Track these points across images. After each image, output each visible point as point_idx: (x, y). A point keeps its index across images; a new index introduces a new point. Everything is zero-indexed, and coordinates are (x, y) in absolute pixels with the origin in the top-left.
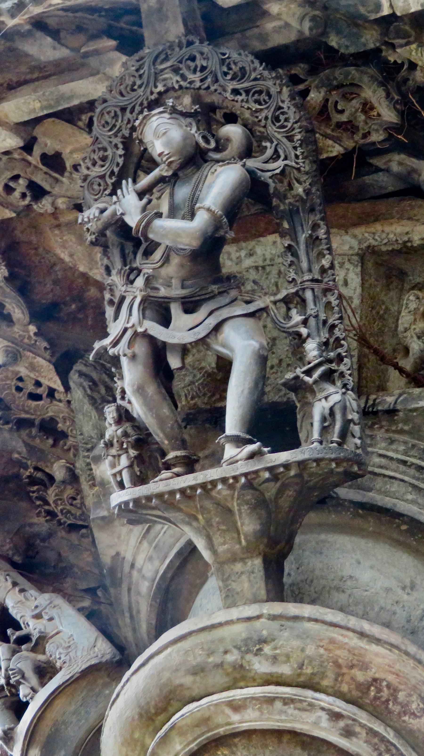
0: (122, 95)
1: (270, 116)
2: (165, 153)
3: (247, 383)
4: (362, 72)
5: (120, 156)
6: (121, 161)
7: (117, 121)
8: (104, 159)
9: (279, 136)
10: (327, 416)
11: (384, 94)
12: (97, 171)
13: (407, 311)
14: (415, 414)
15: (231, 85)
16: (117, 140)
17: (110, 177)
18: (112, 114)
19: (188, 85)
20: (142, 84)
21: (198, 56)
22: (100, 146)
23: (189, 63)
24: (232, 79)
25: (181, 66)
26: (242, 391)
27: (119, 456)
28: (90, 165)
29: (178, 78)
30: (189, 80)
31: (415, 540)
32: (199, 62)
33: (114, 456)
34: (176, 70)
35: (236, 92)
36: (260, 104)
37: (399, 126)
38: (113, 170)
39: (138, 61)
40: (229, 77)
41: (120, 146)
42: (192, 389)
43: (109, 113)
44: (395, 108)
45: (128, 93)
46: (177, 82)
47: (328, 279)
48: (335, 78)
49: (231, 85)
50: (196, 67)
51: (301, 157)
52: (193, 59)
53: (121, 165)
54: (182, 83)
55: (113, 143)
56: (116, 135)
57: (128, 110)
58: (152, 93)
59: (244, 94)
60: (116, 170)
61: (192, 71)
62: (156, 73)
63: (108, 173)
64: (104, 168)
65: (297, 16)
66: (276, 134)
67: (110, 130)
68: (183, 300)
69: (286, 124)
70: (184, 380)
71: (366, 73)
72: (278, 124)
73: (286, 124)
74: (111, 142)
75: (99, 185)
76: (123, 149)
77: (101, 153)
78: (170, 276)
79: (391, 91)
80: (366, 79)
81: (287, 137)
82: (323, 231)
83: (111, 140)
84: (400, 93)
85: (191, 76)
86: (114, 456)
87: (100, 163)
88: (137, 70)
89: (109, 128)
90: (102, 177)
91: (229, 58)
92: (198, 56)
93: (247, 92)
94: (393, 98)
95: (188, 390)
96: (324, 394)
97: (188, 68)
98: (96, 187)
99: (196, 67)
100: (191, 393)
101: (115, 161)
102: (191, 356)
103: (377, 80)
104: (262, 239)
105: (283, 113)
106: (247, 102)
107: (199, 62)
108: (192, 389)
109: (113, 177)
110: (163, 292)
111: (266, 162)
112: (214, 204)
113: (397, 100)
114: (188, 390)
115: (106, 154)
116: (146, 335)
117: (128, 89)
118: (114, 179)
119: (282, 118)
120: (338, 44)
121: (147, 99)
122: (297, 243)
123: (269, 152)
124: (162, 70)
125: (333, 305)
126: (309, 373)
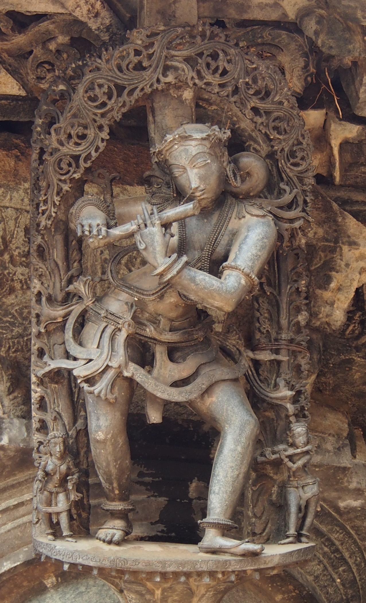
0: (120, 69)
1: (286, 149)
2: (200, 189)
3: (244, 467)
4: (292, 38)
5: (103, 140)
6: (102, 146)
7: (110, 98)
8: (83, 137)
9: (291, 175)
10: (303, 507)
11: (303, 64)
12: (69, 149)
13: (119, 192)
14: (317, 469)
15: (254, 102)
16: (104, 122)
17: (85, 161)
18: (105, 89)
19: (203, 86)
20: (150, 66)
21: (221, 55)
22: (81, 121)
23: (209, 59)
24: (255, 94)
25: (200, 61)
26: (238, 475)
27: (57, 493)
28: (63, 137)
29: (195, 75)
30: (205, 81)
31: (272, 587)
32: (222, 63)
33: (51, 493)
34: (187, 60)
35: (255, 110)
36: (279, 133)
37: (300, 97)
38: (90, 153)
39: (148, 36)
40: (251, 92)
41: (107, 130)
42: (19, 342)
43: (100, 86)
44: (306, 79)
45: (128, 69)
46: (192, 78)
47: (301, 339)
48: (262, 37)
49: (254, 102)
50: (217, 68)
51: (310, 205)
52: (215, 56)
53: (100, 151)
54: (197, 81)
55: (98, 124)
56: (103, 115)
57: (126, 91)
58: (158, 81)
59: (264, 117)
60: (94, 154)
61: (211, 71)
62: (166, 57)
63: (83, 156)
64: (80, 148)
65: (297, 7)
66: (288, 170)
67: (97, 107)
68: (170, 345)
69: (301, 162)
70: (12, 331)
71: (296, 41)
72: (292, 160)
73: (301, 162)
74: (95, 121)
75: (70, 165)
76: (109, 134)
77: (80, 130)
78: (159, 312)
79: (311, 63)
80: (293, 46)
81: (297, 177)
82: (303, 282)
83: (97, 119)
84: (318, 66)
85: (209, 78)
86: (51, 493)
87: (75, 139)
88: (146, 47)
89: (95, 104)
90: (76, 158)
91: (255, 69)
92: (221, 55)
93: (268, 113)
94: (309, 71)
95: (14, 342)
96: (301, 483)
97: (208, 65)
98: (64, 166)
99: (217, 68)
100: (16, 346)
101: (96, 144)
102: (14, 297)
103: (303, 49)
104: (128, 187)
105: (303, 150)
106: (267, 126)
107: (222, 63)
108: (19, 342)
109: (89, 162)
110: (150, 331)
111: (281, 208)
112: (252, 268)
113: (312, 74)
114: (14, 342)
115: (86, 132)
116: (130, 380)
117: (131, 66)
118: (89, 164)
119: (299, 155)
120: (323, 42)
121: (152, 85)
122: (280, 293)
123: (287, 198)
124: (173, 56)
125: (302, 369)
126: (291, 458)
